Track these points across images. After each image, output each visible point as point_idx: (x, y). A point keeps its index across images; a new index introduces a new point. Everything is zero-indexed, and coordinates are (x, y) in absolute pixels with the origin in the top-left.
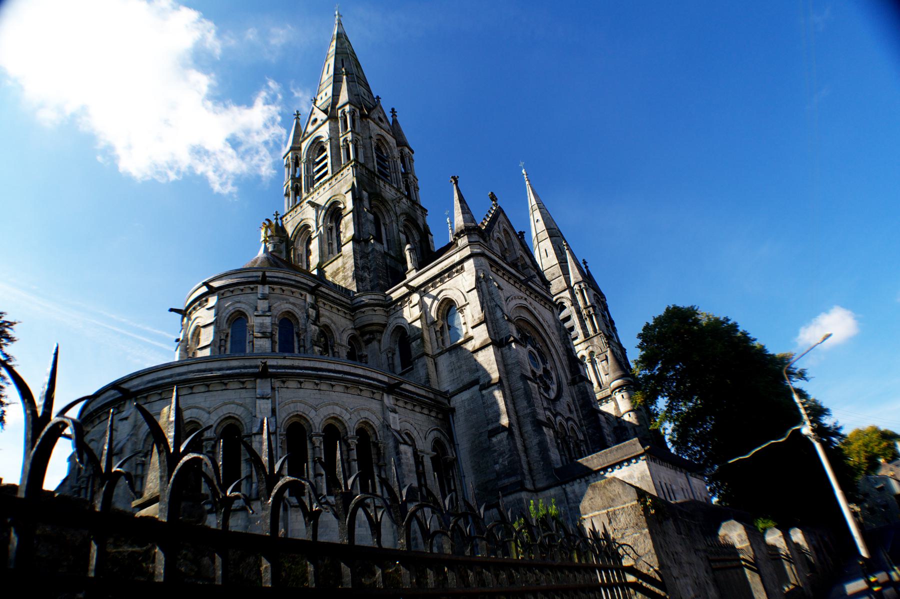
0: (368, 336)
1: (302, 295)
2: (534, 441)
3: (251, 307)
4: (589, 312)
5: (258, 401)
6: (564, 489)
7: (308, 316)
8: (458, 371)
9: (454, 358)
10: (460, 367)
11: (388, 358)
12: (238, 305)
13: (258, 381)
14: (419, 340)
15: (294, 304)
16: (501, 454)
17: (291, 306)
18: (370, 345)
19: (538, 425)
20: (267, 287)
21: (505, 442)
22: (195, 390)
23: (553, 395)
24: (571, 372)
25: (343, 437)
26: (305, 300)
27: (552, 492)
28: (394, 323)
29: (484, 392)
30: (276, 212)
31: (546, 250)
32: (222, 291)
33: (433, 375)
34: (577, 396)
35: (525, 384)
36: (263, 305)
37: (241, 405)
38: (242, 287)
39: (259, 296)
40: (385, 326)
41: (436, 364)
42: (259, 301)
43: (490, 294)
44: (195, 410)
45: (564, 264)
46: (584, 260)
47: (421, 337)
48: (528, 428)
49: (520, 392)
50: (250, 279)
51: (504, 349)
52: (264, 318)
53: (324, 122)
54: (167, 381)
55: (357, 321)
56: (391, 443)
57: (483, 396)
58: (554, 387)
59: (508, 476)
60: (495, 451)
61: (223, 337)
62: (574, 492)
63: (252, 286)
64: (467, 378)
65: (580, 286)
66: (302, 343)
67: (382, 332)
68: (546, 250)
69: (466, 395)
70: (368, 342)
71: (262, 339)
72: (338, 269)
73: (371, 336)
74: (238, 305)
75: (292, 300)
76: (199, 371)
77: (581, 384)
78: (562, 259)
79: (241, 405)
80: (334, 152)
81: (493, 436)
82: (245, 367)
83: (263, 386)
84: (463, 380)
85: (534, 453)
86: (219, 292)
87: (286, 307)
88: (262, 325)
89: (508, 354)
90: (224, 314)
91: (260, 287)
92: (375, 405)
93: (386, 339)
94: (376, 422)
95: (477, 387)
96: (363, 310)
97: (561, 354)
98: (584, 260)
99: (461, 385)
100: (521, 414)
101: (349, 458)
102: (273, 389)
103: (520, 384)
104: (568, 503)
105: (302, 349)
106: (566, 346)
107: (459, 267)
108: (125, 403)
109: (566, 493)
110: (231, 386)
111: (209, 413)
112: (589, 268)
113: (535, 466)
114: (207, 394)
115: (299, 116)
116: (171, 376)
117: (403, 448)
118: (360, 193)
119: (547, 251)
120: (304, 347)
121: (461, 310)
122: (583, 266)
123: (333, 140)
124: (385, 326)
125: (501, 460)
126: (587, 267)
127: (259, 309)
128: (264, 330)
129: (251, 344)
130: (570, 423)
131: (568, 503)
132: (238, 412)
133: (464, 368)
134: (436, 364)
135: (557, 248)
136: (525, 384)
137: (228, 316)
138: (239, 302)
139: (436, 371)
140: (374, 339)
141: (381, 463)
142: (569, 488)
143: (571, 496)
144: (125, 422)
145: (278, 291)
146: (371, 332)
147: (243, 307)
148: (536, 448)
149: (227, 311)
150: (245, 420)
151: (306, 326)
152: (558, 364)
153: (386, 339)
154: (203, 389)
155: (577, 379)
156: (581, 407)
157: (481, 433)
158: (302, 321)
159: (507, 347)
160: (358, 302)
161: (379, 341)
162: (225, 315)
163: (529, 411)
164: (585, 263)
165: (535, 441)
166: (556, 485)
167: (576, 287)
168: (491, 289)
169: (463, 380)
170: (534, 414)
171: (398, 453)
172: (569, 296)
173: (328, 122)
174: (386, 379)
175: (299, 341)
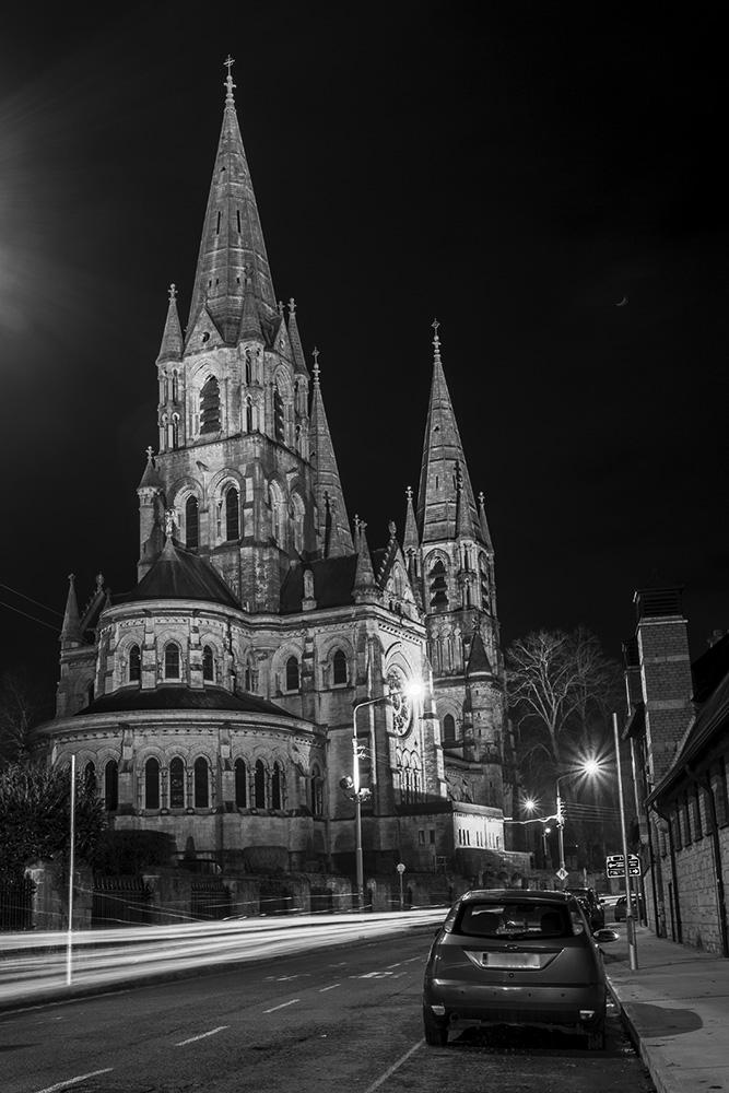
5: (223, 747)
23: (404, 730)
27: (390, 819)
33: (317, 709)
47: (312, 674)
56: (293, 774)
58: (407, 724)
62: (404, 823)
70: (262, 659)
72: (231, 565)
74: (173, 634)
82: (213, 721)
83: (224, 733)
88: (195, 658)
113: (382, 800)
117: (302, 778)
121: (351, 660)
123: (229, 382)
130: (414, 755)
133: (343, 711)
142: (401, 819)
143: (402, 825)
146: (265, 652)
156: (426, 740)
158: (219, 650)
162: (162, 641)
166: (395, 815)
171: (298, 782)
172: (450, 552)
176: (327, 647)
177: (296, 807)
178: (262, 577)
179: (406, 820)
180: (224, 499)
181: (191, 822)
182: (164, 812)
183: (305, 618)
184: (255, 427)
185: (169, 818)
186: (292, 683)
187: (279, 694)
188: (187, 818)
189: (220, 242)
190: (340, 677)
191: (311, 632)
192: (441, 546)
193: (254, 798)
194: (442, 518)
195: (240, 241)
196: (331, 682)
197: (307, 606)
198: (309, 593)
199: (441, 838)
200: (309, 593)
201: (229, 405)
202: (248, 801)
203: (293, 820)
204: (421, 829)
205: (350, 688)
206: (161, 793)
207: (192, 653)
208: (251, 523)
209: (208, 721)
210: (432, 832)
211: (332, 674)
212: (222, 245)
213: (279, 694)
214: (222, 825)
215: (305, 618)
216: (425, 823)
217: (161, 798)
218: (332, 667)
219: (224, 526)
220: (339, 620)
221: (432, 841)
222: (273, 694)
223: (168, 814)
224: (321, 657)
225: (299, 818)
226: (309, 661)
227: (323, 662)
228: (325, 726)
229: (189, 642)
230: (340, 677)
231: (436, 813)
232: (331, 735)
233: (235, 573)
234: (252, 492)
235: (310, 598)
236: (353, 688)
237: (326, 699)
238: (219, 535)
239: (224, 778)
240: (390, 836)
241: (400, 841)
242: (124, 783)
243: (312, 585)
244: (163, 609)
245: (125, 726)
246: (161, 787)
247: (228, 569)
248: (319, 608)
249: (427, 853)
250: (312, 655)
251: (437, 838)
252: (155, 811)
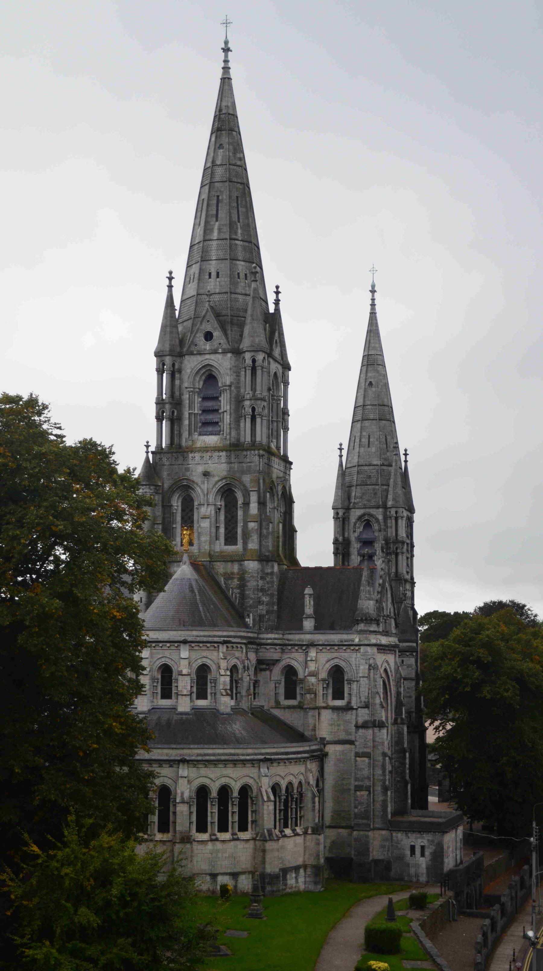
0: (264, 666)
1: (241, 647)
2: (380, 798)
3: (214, 663)
4: (397, 549)
6: (392, 834)
7: (244, 667)
8: (336, 728)
9: (335, 716)
10: (339, 725)
11: (276, 687)
12: (204, 660)
13: (261, 763)
14: (313, 695)
15: (237, 658)
16: (361, 803)
17: (236, 660)
18: (263, 673)
19: (385, 789)
20: (225, 646)
21: (365, 797)
22: (228, 766)
24: (395, 712)
25: (291, 792)
26: (242, 652)
27: (384, 832)
28: (288, 660)
29: (358, 759)
30: (148, 442)
31: (369, 436)
32: (193, 645)
34: (395, 733)
35: (384, 759)
36: (223, 664)
37: (252, 778)
38: (209, 645)
39: (221, 655)
40: (278, 661)
41: (319, 714)
42: (222, 661)
43: (375, 681)
44: (227, 778)
45: (385, 468)
46: (406, 450)
48: (379, 788)
49: (380, 764)
50: (216, 639)
51: (375, 729)
52: (226, 677)
53: (224, 352)
54: (212, 758)
55: (261, 654)
56: (309, 795)
57: (356, 761)
59: (363, 818)
60: (357, 800)
61: (192, 685)
62: (397, 837)
63: (216, 645)
64: (343, 736)
65: (396, 512)
66: (239, 690)
67: (274, 664)
68: (369, 436)
69: (339, 748)
71: (226, 697)
72: (233, 573)
73: (267, 667)
74: (204, 660)
75: (238, 654)
76: (231, 754)
77: (401, 726)
78: (385, 459)
79: (252, 778)
80: (233, 407)
81: (358, 791)
84: (339, 736)
85: (378, 806)
86: (190, 644)
87: (234, 661)
88: (225, 682)
89: (378, 734)
90: (194, 665)
91: (221, 645)
92: (302, 769)
93: (277, 670)
94: (303, 782)
95: (348, 746)
96: (268, 647)
97: (393, 696)
98: (406, 450)
99: (337, 739)
100: (376, 777)
101: (291, 805)
102: (268, 769)
103: (380, 758)
104: (392, 842)
105: (238, 695)
106: (398, 689)
107: (357, 648)
108: (179, 764)
109: (392, 836)
110: (247, 765)
111: (236, 781)
112: (408, 463)
113: (377, 813)
114: (234, 769)
115: (173, 281)
116: (214, 755)
118: (265, 496)
119: (371, 440)
120: (240, 693)
121: (350, 682)
122: (403, 458)
123: (233, 388)
124: (278, 661)
125: (359, 807)
126: (406, 461)
127: (221, 667)
128: (226, 687)
129: (213, 694)
131: (392, 842)
132: (250, 782)
133: (342, 727)
134: (319, 714)
135: (384, 440)
136: (384, 759)
137: (196, 667)
138: (206, 657)
139: (319, 719)
140: (268, 669)
141: (302, 805)
142: (394, 834)
143: (394, 838)
144: (184, 779)
145: (230, 649)
147: (208, 662)
148: (381, 803)
149: (196, 663)
150: (254, 788)
151: (242, 676)
152: (389, 708)
153: (277, 670)
154: (231, 765)
155: (399, 720)
157: (345, 778)
158: (240, 671)
159: (378, 729)
160: (263, 639)
161: (271, 671)
162: (195, 666)
163: (382, 778)
164: (406, 455)
165: (381, 798)
167: (393, 512)
168: (376, 676)
169: (339, 736)
170: (384, 781)
171: (314, 803)
172: (380, 517)
173: (229, 355)
174: (307, 748)
175: (237, 687)
176: (328, 666)
177: (310, 825)
178: (262, 590)
179: (400, 835)
180: (223, 503)
181: (236, 847)
182: (213, 837)
183: (308, 637)
184: (258, 439)
185: (218, 843)
186: (290, 694)
187: (278, 705)
188: (232, 843)
189: (220, 230)
190: (338, 694)
191: (313, 653)
192: (373, 511)
193: (282, 821)
194: (374, 480)
195: (239, 231)
196: (330, 697)
197: (308, 624)
198: (309, 609)
199: (431, 853)
200: (309, 609)
201: (232, 411)
202: (278, 823)
203: (309, 837)
204: (413, 844)
205: (348, 708)
206: (209, 819)
207: (222, 679)
208: (255, 537)
209: (252, 754)
210: (423, 848)
211: (330, 691)
212: (223, 236)
213: (278, 705)
214: (264, 851)
215: (308, 637)
216: (417, 838)
217: (209, 824)
218: (331, 684)
219: (222, 530)
220: (340, 645)
221: (423, 855)
222: (273, 703)
223: (217, 840)
224: (323, 675)
225: (314, 836)
226: (313, 680)
227: (324, 680)
228: (323, 739)
229: (219, 667)
230: (338, 694)
231: (428, 832)
232: (330, 749)
233: (236, 582)
234: (256, 505)
235: (309, 617)
236: (352, 709)
237: (326, 715)
238: (217, 538)
239: (265, 807)
240: (383, 847)
241: (392, 852)
242: (182, 812)
243: (312, 603)
244: (198, 636)
245: (183, 761)
246: (209, 814)
247: (229, 577)
248: (318, 628)
249: (417, 866)
250: (312, 674)
251: (427, 853)
252: (205, 837)
